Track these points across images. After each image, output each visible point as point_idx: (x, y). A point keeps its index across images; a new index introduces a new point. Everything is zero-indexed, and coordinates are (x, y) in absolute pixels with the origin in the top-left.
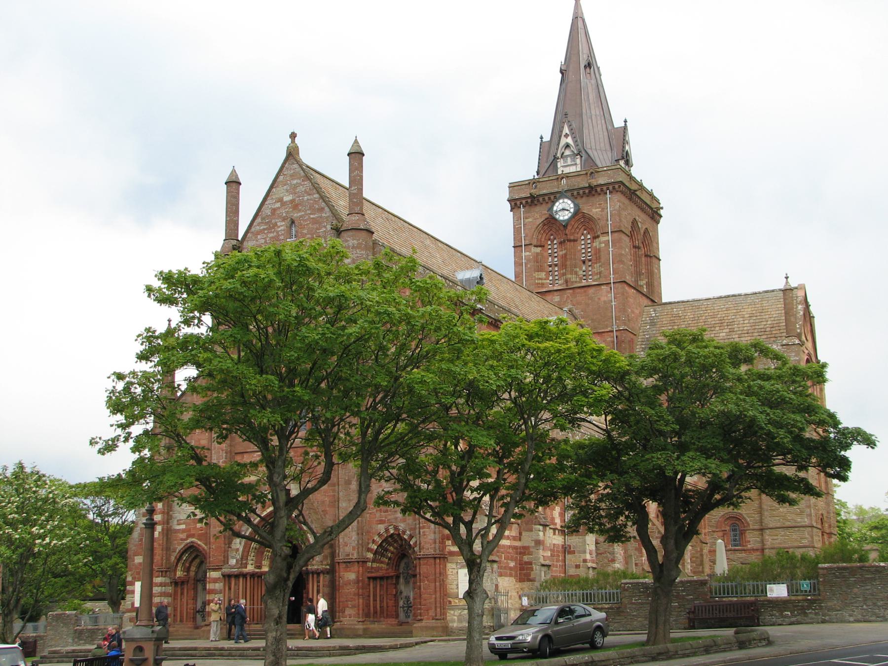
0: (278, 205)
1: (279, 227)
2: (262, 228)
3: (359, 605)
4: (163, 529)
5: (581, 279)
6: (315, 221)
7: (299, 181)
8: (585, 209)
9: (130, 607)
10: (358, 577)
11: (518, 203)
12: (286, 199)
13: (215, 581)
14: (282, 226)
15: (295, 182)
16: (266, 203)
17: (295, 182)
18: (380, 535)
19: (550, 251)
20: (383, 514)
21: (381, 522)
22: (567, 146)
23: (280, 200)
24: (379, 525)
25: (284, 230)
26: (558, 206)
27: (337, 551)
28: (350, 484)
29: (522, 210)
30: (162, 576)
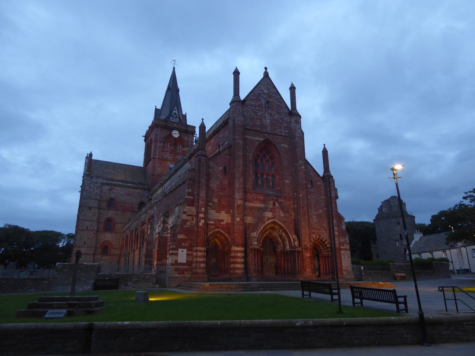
0: (261, 92)
1: (262, 101)
2: (254, 98)
3: (312, 267)
4: (205, 222)
7: (270, 87)
10: (310, 255)
11: (159, 126)
12: (265, 91)
13: (238, 252)
14: (263, 102)
16: (255, 89)
18: (313, 239)
19: (166, 146)
20: (314, 230)
21: (314, 233)
22: (175, 113)
23: (262, 91)
24: (313, 235)
25: (264, 103)
26: (174, 132)
27: (301, 243)
30: (204, 247)
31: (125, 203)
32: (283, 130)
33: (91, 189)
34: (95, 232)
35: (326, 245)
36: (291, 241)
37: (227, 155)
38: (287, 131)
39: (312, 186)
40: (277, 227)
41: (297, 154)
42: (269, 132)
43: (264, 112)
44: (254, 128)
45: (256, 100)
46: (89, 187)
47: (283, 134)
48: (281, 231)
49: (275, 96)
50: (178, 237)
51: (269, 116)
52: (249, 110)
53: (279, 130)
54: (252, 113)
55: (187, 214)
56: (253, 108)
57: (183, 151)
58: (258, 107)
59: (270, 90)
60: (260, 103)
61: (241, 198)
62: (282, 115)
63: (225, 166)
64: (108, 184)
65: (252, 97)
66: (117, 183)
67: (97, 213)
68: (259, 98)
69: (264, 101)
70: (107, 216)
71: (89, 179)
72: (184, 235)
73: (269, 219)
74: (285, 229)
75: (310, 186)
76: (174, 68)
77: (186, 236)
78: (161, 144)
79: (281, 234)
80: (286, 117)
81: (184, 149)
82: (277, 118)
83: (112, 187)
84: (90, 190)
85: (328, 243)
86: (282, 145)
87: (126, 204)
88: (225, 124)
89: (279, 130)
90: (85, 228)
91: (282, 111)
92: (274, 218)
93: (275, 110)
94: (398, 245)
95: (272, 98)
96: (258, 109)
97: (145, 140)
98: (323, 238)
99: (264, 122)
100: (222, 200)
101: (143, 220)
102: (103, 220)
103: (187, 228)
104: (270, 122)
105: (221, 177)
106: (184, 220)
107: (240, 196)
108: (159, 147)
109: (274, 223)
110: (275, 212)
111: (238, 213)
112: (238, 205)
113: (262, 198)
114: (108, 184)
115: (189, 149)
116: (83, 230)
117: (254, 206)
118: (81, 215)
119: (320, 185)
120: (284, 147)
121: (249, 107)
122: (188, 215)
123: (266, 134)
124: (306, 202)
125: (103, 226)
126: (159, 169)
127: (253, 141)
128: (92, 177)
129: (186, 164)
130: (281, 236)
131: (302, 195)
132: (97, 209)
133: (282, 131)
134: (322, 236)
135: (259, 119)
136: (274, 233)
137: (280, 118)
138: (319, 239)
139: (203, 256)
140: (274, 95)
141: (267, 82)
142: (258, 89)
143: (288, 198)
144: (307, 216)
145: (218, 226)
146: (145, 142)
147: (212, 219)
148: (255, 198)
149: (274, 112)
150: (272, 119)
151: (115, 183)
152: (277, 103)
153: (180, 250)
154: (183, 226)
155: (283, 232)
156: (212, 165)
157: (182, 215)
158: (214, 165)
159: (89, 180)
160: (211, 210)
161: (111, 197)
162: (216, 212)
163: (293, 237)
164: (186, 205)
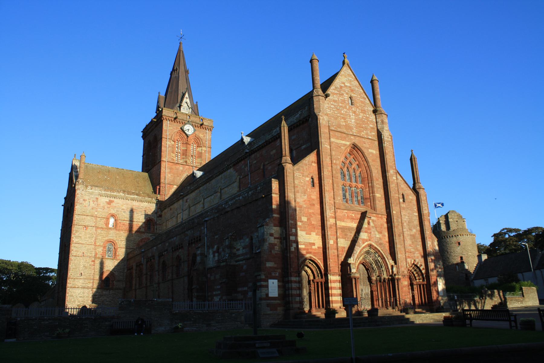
0: (343, 85)
1: (345, 96)
2: (336, 92)
5: (191, 163)
6: (362, 102)
7: (352, 79)
8: (197, 133)
9: (264, 296)
12: (346, 84)
13: (335, 281)
14: (346, 97)
15: (350, 78)
17: (350, 78)
21: (409, 257)
28: (400, 236)
29: (168, 122)
32: (369, 132)
33: (85, 202)
34: (93, 259)
35: (420, 271)
36: (388, 268)
37: (312, 162)
38: (374, 134)
39: (404, 201)
40: (371, 250)
41: (388, 162)
42: (355, 134)
43: (348, 110)
44: (339, 130)
45: (338, 95)
46: (84, 200)
47: (370, 137)
48: (376, 255)
49: (358, 90)
50: (267, 265)
51: (354, 115)
52: (332, 106)
53: (365, 132)
54: (336, 111)
55: (274, 236)
56: (336, 104)
57: (199, 152)
58: (342, 103)
59: (352, 83)
60: (343, 99)
61: (333, 216)
62: (367, 113)
63: (312, 177)
65: (334, 91)
67: (95, 234)
68: (342, 92)
69: (347, 96)
70: (106, 238)
71: (83, 189)
72: (273, 263)
73: (364, 241)
74: (381, 253)
75: (401, 200)
77: (275, 264)
78: (170, 142)
79: (376, 259)
80: (371, 117)
82: (363, 117)
83: (111, 199)
84: (84, 203)
85: (424, 269)
86: (370, 150)
88: (301, 122)
89: (365, 132)
90: (81, 254)
91: (366, 108)
92: (370, 240)
93: (360, 108)
94: (459, 269)
95: (355, 92)
96: (341, 106)
97: (144, 137)
98: (418, 263)
99: (349, 122)
100: (312, 218)
101: (177, 243)
102: (102, 244)
103: (276, 254)
104: (356, 122)
105: (308, 190)
106: (271, 244)
107: (332, 213)
108: (169, 146)
109: (370, 246)
110: (371, 233)
111: (331, 235)
112: (330, 225)
113: (353, 215)
115: (205, 149)
116: (78, 256)
117: (345, 225)
118: (74, 237)
119: (411, 199)
120: (372, 153)
121: (332, 103)
122: (275, 238)
123: (352, 137)
124: (400, 220)
125: (102, 251)
126: (169, 175)
127: (339, 145)
128: (87, 187)
129: (229, 171)
130: (377, 262)
131: (396, 212)
132: (94, 228)
133: (368, 133)
134: (417, 260)
135: (343, 118)
136: (369, 258)
137: (365, 118)
138: (413, 264)
139: (298, 287)
140: (357, 89)
141: (348, 73)
142: (339, 81)
143: (380, 215)
144: (402, 237)
145: (310, 251)
146: (143, 139)
147: (302, 242)
148: (346, 215)
149: (358, 109)
150: (357, 118)
152: (361, 98)
153: (271, 281)
154: (271, 251)
155: (380, 257)
156: (299, 175)
157: (268, 238)
158: (300, 175)
159: (83, 190)
160: (300, 232)
161: (111, 212)
162: (306, 234)
163: (390, 262)
164: (272, 225)
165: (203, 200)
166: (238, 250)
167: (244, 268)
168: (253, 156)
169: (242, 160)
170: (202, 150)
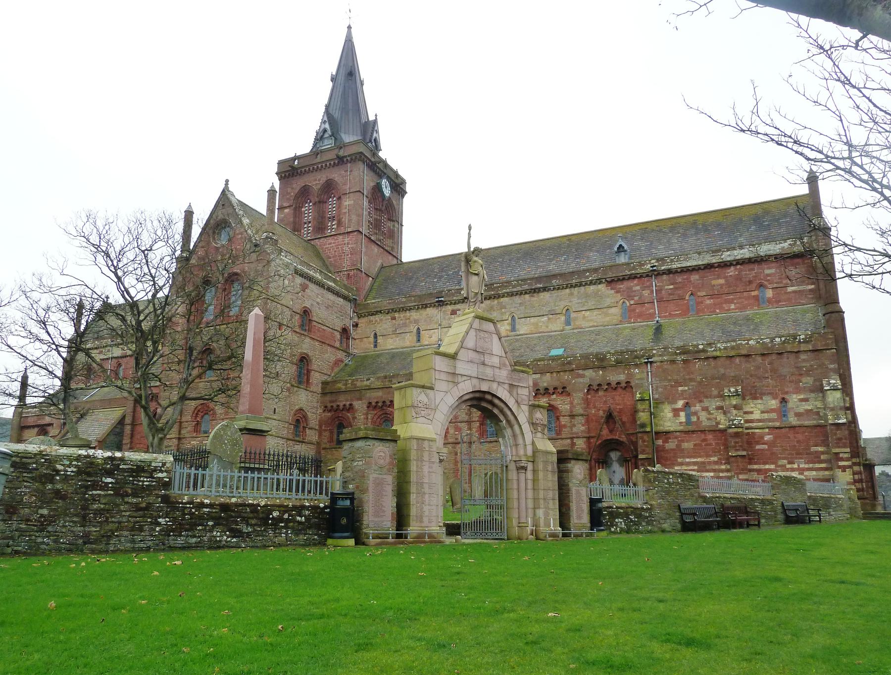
31: (324, 325)
57: (389, 228)
64: (302, 275)
66: (315, 275)
76: (349, 27)
81: (390, 224)
83: (307, 282)
87: (325, 328)
114: (302, 275)
128: (281, 250)
151: (311, 273)
165: (510, 319)
166: (752, 413)
167: (766, 439)
168: (665, 277)
169: (635, 277)
170: (394, 226)
